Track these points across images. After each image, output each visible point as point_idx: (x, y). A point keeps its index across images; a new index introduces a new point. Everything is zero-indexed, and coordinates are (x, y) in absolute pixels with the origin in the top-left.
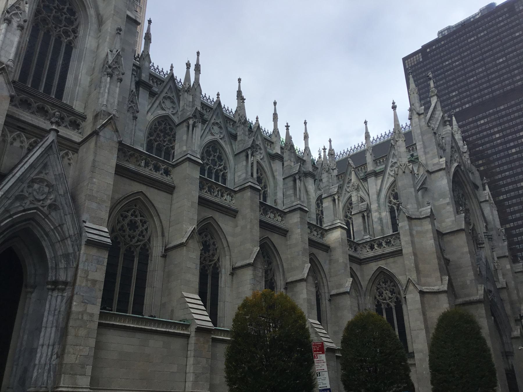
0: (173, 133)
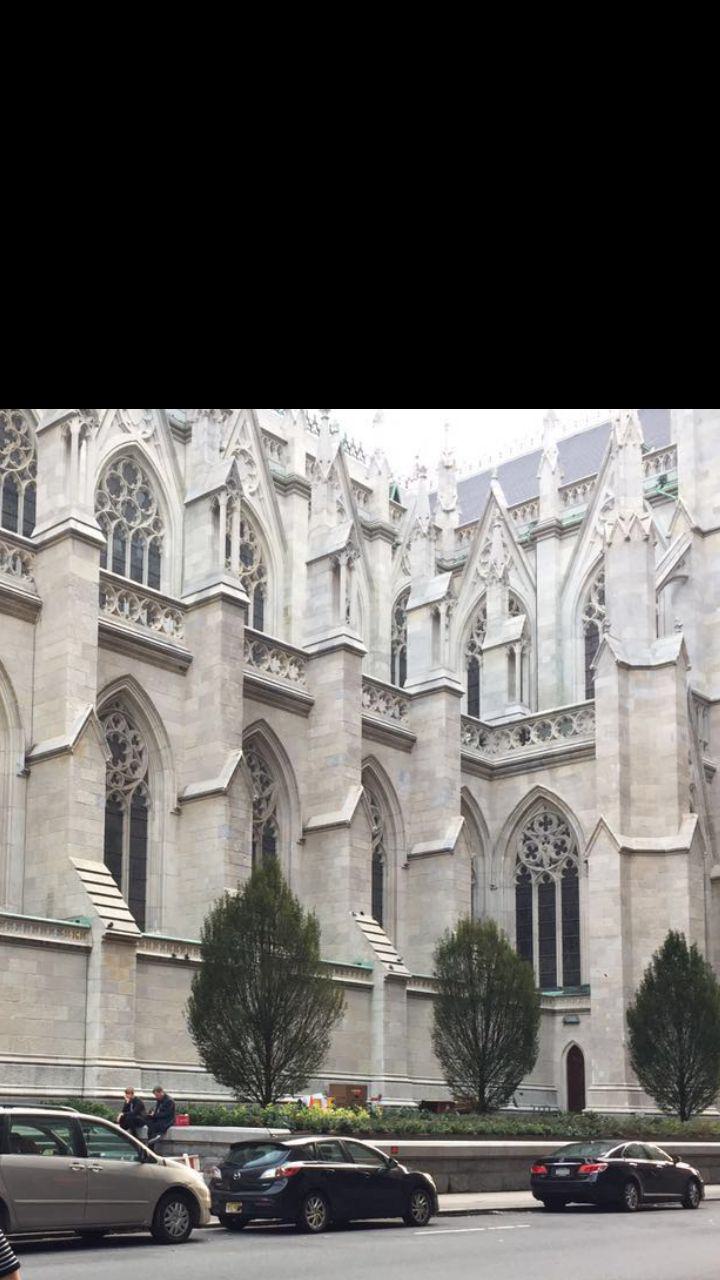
0: (22, 432)
